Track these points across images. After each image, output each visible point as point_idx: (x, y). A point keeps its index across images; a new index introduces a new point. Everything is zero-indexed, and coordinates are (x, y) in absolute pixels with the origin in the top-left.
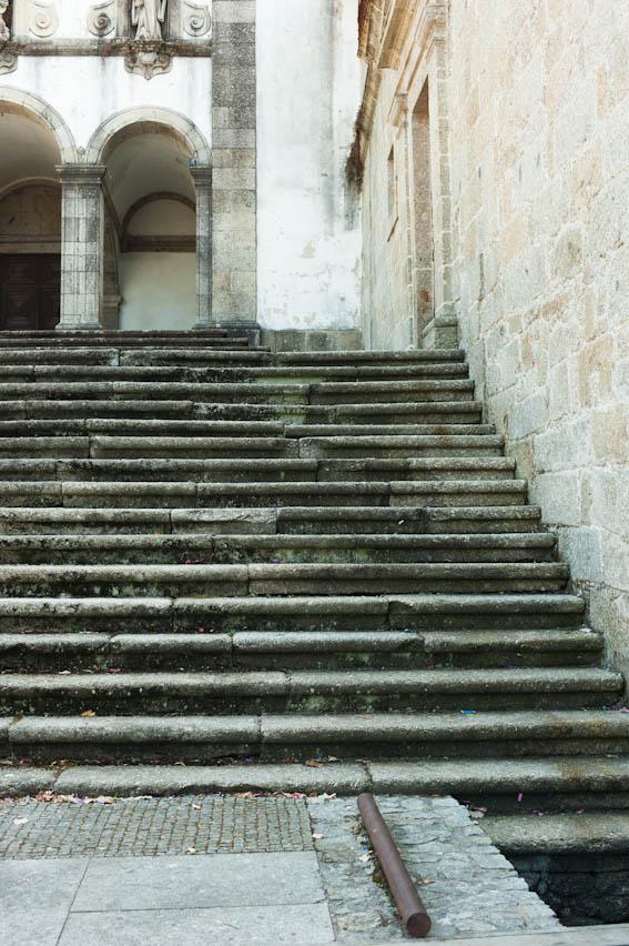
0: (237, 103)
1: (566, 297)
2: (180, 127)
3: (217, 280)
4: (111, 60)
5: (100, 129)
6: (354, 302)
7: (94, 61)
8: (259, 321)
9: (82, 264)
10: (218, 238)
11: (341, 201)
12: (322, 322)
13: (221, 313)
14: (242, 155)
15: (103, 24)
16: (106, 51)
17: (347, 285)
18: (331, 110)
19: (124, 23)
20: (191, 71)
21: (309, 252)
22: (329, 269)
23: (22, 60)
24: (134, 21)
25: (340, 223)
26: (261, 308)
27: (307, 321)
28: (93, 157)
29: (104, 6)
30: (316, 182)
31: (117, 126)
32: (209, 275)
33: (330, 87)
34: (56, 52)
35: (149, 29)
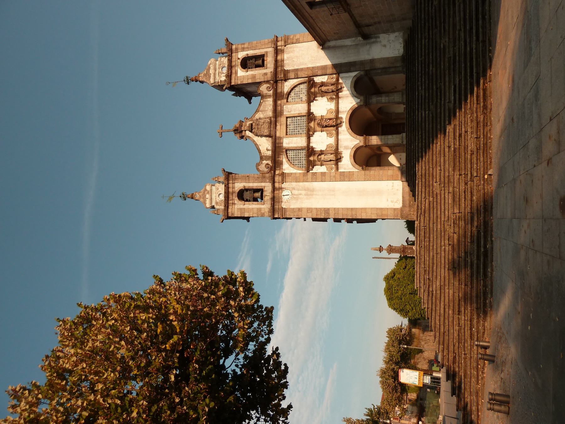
2: (355, 79)
4: (340, 96)
6: (397, 34)
7: (339, 99)
8: (401, 55)
9: (387, 98)
10: (381, 66)
11: (372, 40)
12: (401, 40)
14: (362, 63)
15: (332, 99)
16: (338, 97)
17: (392, 36)
18: (351, 45)
19: (331, 94)
21: (385, 46)
22: (389, 41)
23: (340, 116)
24: (331, 91)
25: (378, 40)
26: (398, 55)
27: (401, 44)
28: (362, 98)
29: (328, 99)
30: (368, 47)
31: (355, 93)
32: (390, 68)
33: (346, 46)
34: (338, 108)
35: (333, 88)
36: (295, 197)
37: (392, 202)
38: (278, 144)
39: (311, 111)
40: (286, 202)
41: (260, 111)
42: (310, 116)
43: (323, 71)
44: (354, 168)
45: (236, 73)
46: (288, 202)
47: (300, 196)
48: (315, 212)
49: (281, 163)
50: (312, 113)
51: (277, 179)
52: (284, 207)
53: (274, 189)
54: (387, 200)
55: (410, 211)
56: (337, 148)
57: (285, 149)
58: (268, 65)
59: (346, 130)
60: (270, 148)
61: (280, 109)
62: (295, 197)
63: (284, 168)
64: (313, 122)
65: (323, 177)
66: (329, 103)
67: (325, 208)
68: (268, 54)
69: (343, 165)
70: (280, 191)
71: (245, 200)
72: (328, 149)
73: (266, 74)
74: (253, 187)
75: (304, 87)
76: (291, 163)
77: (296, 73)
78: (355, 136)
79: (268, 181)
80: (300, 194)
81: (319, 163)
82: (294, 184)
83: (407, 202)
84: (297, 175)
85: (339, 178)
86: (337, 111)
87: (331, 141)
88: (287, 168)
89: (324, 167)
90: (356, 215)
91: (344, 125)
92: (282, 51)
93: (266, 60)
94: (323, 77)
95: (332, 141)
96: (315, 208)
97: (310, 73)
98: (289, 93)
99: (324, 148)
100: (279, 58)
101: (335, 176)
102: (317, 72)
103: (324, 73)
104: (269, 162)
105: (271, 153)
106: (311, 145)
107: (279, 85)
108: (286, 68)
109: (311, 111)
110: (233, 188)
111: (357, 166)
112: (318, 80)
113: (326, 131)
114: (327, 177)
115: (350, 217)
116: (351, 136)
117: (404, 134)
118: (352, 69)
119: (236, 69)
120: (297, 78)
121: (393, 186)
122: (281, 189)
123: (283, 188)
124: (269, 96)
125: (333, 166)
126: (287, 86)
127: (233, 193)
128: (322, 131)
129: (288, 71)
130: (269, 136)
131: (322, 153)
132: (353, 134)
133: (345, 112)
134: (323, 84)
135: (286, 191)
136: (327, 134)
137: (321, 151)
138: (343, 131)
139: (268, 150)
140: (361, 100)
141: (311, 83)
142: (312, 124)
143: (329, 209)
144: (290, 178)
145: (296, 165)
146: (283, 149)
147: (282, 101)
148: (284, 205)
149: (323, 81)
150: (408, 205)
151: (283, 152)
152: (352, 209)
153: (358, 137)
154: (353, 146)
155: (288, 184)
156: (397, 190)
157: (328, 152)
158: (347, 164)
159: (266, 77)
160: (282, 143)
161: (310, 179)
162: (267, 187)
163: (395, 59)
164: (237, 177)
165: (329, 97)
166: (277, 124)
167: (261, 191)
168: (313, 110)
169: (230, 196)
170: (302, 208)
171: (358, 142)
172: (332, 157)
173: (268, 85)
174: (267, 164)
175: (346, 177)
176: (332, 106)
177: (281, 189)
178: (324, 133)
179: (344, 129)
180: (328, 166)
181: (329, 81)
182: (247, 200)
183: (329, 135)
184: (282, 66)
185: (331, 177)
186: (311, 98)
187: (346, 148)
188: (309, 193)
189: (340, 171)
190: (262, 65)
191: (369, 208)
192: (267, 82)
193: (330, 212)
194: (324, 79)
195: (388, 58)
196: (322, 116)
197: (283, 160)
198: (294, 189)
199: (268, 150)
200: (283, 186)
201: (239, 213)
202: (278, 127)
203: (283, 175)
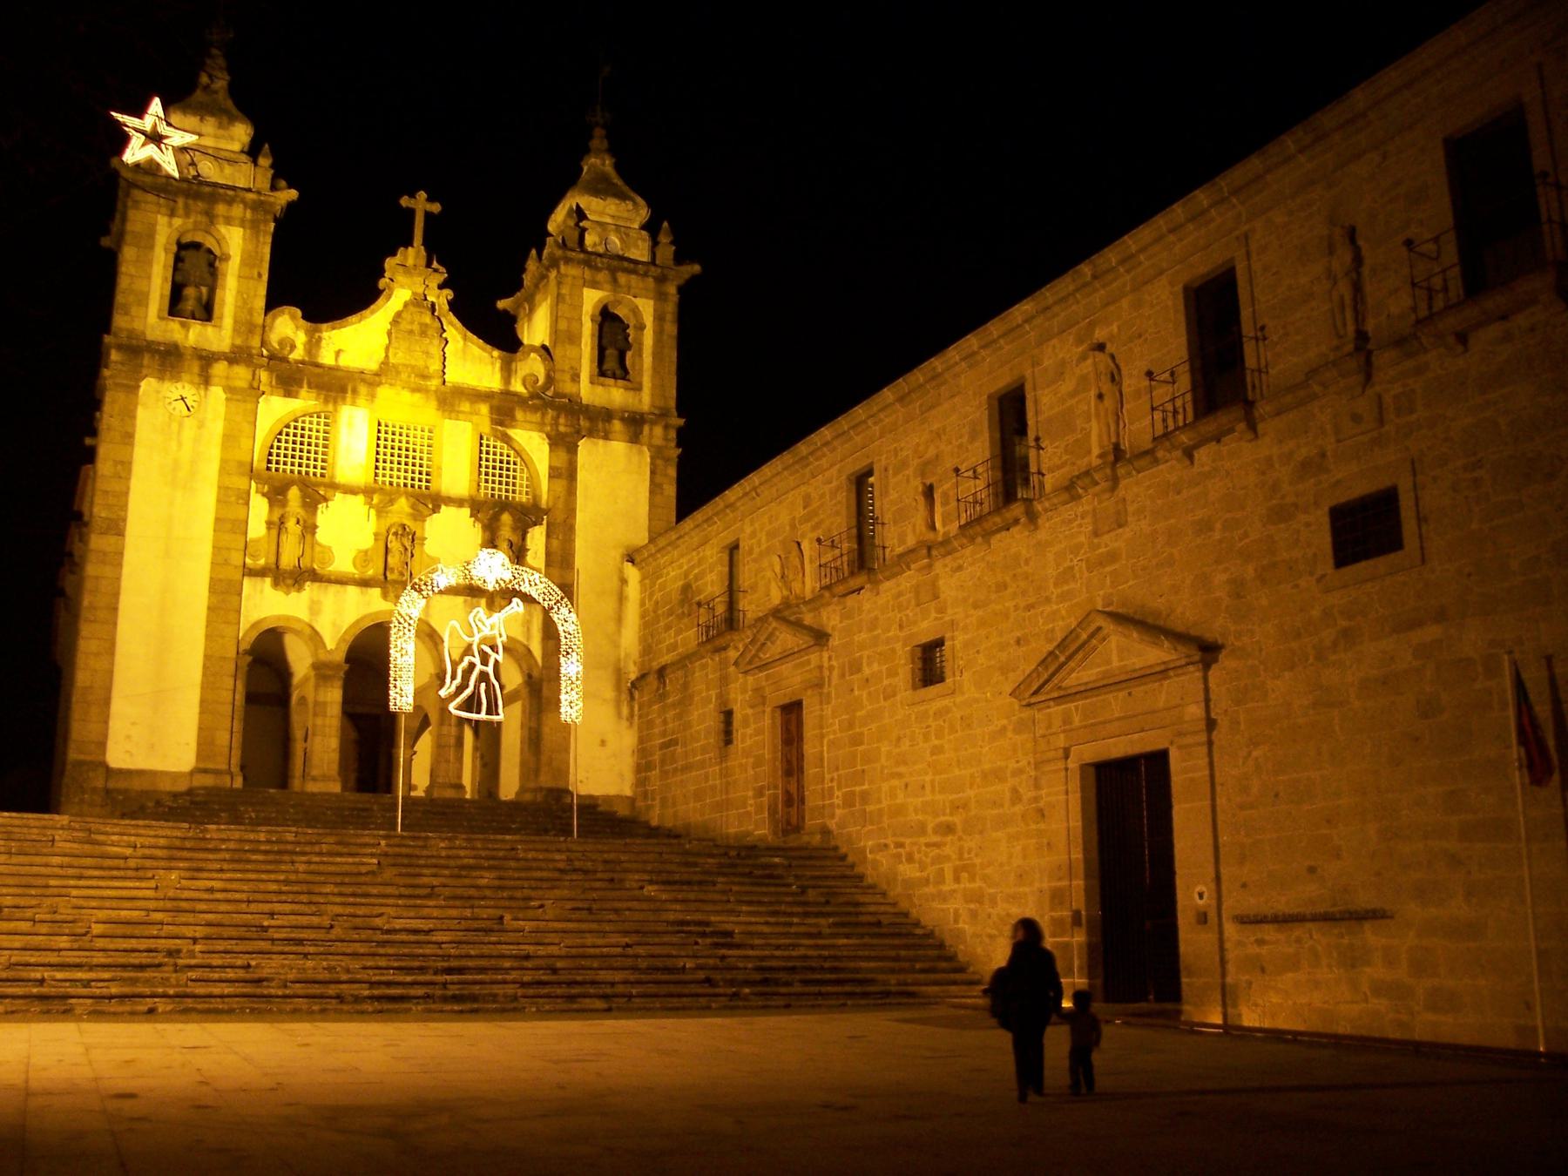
1: (945, 844)
3: (544, 759)
6: (629, 777)
13: (546, 780)
25: (625, 724)
26: (572, 778)
33: (619, 632)
36: (175, 426)
38: (355, 391)
39: (443, 507)
40: (158, 392)
42: (431, 501)
44: (248, 626)
45: (594, 285)
46: (158, 400)
47: (174, 445)
49: (289, 394)
50: (436, 510)
51: (241, 374)
52: (143, 384)
53: (206, 359)
54: (133, 724)
55: (94, 790)
56: (315, 577)
60: (344, 361)
61: (462, 409)
62: (175, 426)
64: (410, 511)
65: (230, 524)
67: (124, 520)
68: (631, 394)
69: (262, 591)
70: (197, 379)
71: (183, 253)
72: (317, 549)
73: (576, 378)
74: (224, 288)
77: (566, 474)
78: (350, 639)
79: (238, 342)
80: (180, 444)
81: (275, 518)
82: (216, 428)
83: (122, 784)
84: (245, 443)
85: (221, 576)
88: (275, 409)
92: (634, 439)
93: (616, 386)
95: (343, 564)
96: (128, 488)
98: (507, 440)
99: (321, 536)
100: (617, 425)
101: (226, 562)
102: (558, 538)
104: (298, 354)
106: (339, 496)
107: (537, 417)
108: (584, 446)
109: (443, 507)
110: (229, 221)
111: (254, 634)
113: (374, 548)
116: (350, 627)
117: (336, 788)
119: (607, 286)
122: (206, 381)
123: (206, 389)
126: (533, 443)
127: (211, 217)
128: (376, 535)
129: (572, 450)
130: (385, 363)
131: (309, 529)
132: (357, 631)
136: (366, 552)
137: (315, 527)
139: (338, 353)
143: (121, 533)
145: (279, 441)
146: (335, 402)
148: (148, 385)
149: (529, 553)
150: (111, 785)
151: (326, 401)
152: (114, 609)
153: (345, 648)
154: (318, 628)
155: (222, 409)
157: (308, 549)
159: (567, 377)
160: (353, 404)
162: (218, 336)
163: (563, 772)
164: (261, 239)
166: (417, 396)
167: (206, 312)
169: (201, 205)
170: (132, 445)
172: (288, 560)
173: (541, 381)
174: (293, 347)
175: (224, 596)
177: (206, 381)
178: (367, 542)
182: (178, 259)
183: (364, 557)
184: (591, 434)
187: (315, 608)
189: (247, 582)
190: (602, 371)
191: (112, 663)
192: (550, 379)
193: (112, 539)
195: (567, 750)
196: (425, 539)
199: (338, 353)
200: (217, 393)
203: (255, 392)
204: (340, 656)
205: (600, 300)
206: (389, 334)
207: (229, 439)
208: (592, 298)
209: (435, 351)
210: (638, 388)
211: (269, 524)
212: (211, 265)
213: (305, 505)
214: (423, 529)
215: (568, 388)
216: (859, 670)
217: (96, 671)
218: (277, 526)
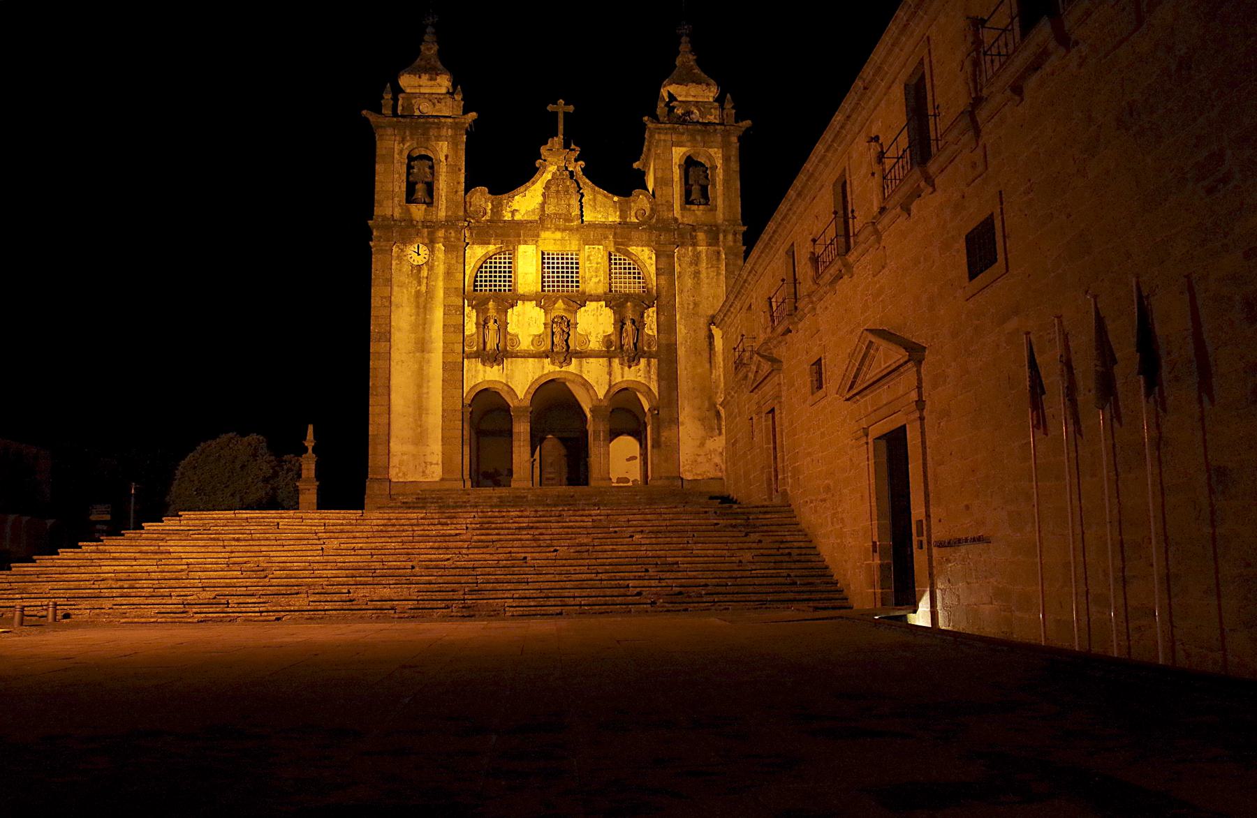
0: (668, 377)
5: (608, 391)
20: (649, 364)
21: (702, 445)
37: (401, 463)
41: (595, 195)
43: (667, 327)
44: (469, 389)
48: (384, 312)
57: (514, 248)
58: (687, 214)
59: (546, 372)
60: (518, 217)
63: (475, 246)
66: (600, 338)
72: (509, 337)
75: (633, 288)
76: (485, 262)
79: (450, 213)
82: (440, 269)
86: (583, 355)
87: (525, 344)
88: (476, 253)
89: (474, 330)
90: (376, 395)
91: (558, 369)
94: (655, 327)
97: (664, 300)
98: (628, 254)
102: (664, 314)
103: (661, 327)
105: (506, 218)
112: (651, 316)
113: (545, 333)
114: (452, 337)
115: (373, 384)
118: (663, 383)
119: (689, 144)
120: (657, 275)
121: (431, 464)
124: (623, 215)
125: (475, 349)
128: (545, 324)
133: (581, 371)
134: (639, 325)
135: (427, 252)
138: (543, 367)
140: (600, 400)
141: (644, 300)
142: (560, 304)
144: (453, 261)
145: (481, 272)
147: (612, 244)
153: (530, 397)
156: (424, 472)
158: (480, 375)
160: (526, 243)
161: (449, 301)
165: (613, 338)
168: (591, 306)
171: (521, 395)
175: (453, 372)
176: (595, 344)
179: (549, 368)
180: (475, 336)
181: (646, 338)
183: (538, 339)
185: (451, 345)
186: (615, 301)
188: (422, 299)
190: (688, 200)
194: (651, 328)
197: (491, 246)
198: (431, 269)
199: (513, 212)
201: (384, 152)
202: (558, 235)
204: (527, 403)
205: (684, 153)
206: (544, 195)
207: (449, 274)
208: (678, 153)
209: (574, 202)
210: (714, 209)
211: (477, 324)
212: (432, 167)
213: (498, 311)
214: (575, 318)
215: (667, 215)
216: (794, 385)
217: (379, 424)
218: (482, 325)
